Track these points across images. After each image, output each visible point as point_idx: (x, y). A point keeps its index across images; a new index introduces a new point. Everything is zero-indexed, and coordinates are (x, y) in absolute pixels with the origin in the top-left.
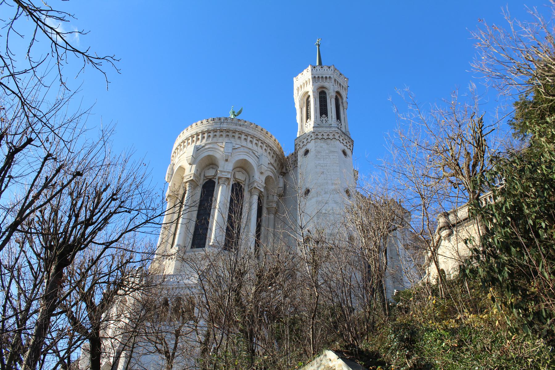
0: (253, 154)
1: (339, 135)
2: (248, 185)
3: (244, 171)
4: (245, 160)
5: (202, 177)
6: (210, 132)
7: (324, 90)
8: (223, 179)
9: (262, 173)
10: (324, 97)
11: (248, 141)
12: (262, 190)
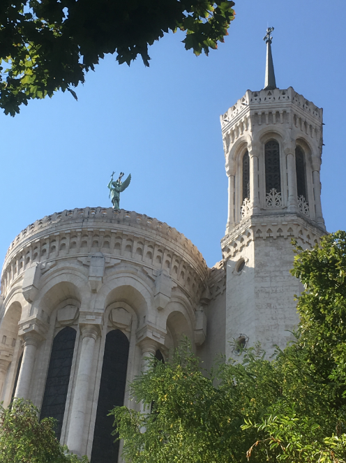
0: (144, 277)
1: (299, 228)
2: (137, 333)
3: (128, 307)
4: (129, 286)
5: (53, 323)
6: (64, 238)
7: (274, 138)
8: (89, 327)
9: (160, 309)
10: (275, 151)
11: (134, 250)
12: (162, 341)
